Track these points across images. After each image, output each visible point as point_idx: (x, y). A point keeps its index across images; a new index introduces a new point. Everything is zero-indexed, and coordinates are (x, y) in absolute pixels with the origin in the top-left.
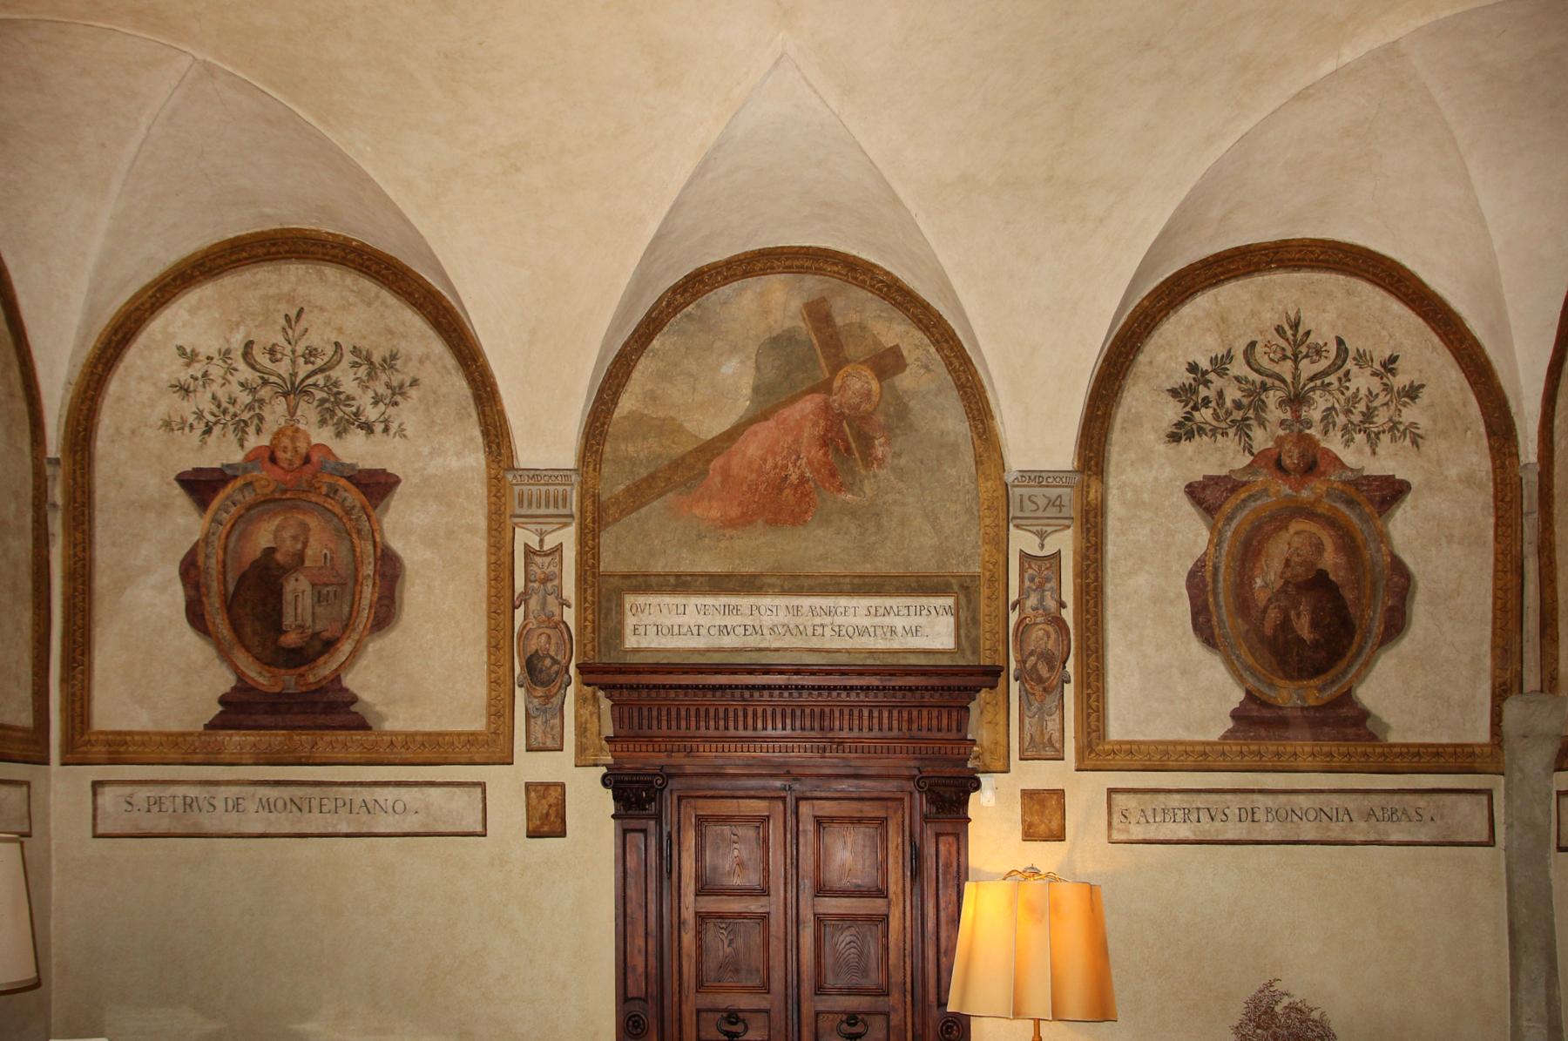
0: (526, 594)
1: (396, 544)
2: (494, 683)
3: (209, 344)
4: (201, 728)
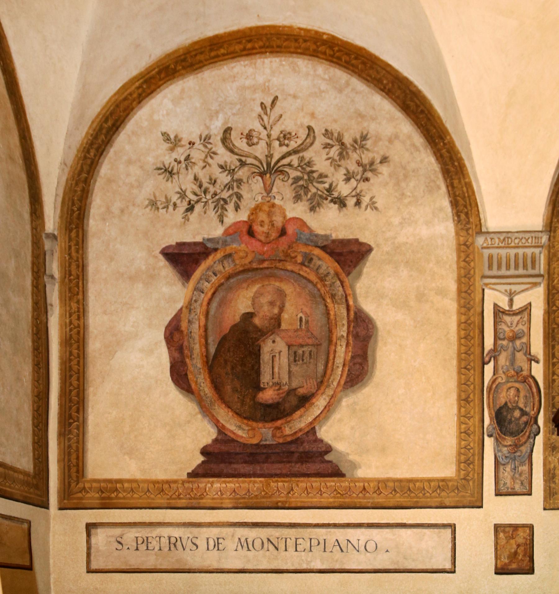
0: (495, 353)
1: (369, 307)
2: (464, 433)
3: (191, 131)
4: (185, 477)
